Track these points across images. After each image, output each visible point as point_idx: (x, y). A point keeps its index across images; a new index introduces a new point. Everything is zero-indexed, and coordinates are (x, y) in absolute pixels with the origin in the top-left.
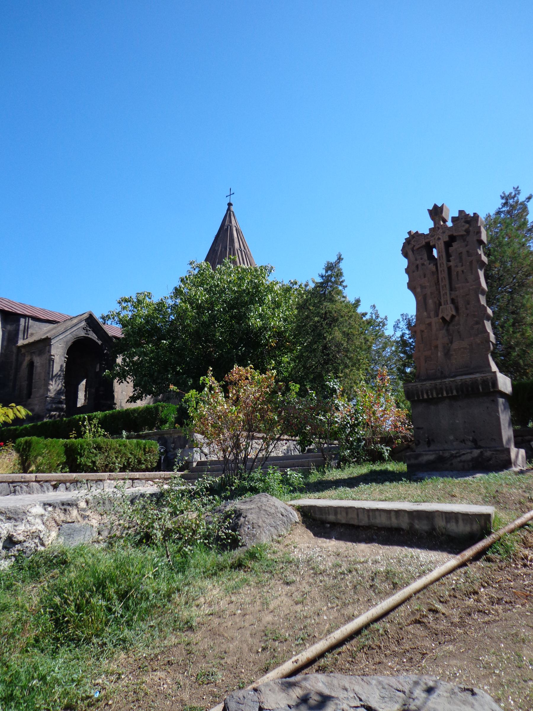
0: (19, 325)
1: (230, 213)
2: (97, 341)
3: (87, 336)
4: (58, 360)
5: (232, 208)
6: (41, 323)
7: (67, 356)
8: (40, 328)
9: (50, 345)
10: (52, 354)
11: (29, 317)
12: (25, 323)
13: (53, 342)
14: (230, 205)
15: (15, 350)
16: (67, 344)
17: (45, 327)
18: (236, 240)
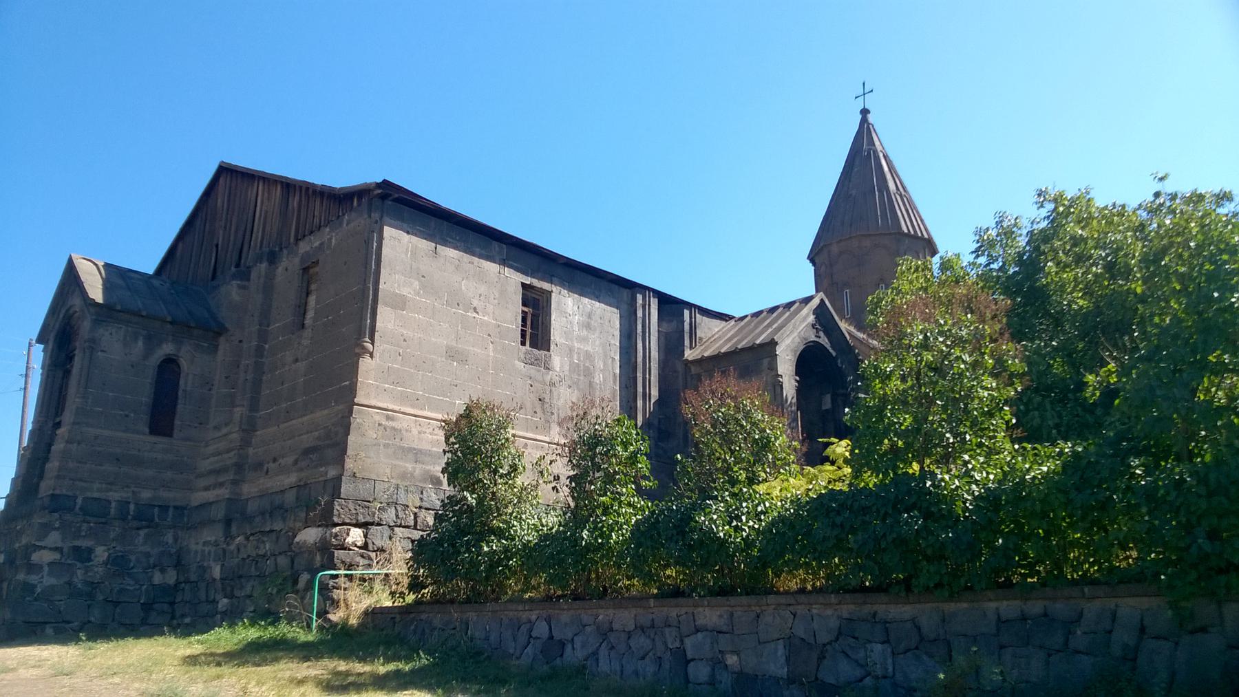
0: (683, 322)
1: (868, 127)
2: (831, 351)
3: (817, 340)
4: (787, 385)
5: (871, 118)
6: (710, 320)
7: (798, 378)
8: (709, 329)
9: (774, 356)
10: (779, 373)
11: (696, 306)
12: (691, 318)
13: (779, 350)
14: (865, 112)
15: (680, 368)
16: (795, 354)
17: (716, 326)
18: (889, 176)
